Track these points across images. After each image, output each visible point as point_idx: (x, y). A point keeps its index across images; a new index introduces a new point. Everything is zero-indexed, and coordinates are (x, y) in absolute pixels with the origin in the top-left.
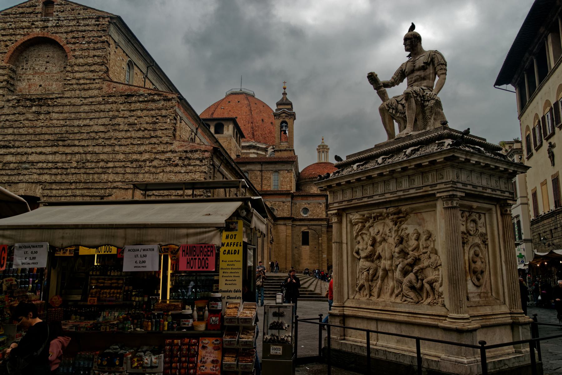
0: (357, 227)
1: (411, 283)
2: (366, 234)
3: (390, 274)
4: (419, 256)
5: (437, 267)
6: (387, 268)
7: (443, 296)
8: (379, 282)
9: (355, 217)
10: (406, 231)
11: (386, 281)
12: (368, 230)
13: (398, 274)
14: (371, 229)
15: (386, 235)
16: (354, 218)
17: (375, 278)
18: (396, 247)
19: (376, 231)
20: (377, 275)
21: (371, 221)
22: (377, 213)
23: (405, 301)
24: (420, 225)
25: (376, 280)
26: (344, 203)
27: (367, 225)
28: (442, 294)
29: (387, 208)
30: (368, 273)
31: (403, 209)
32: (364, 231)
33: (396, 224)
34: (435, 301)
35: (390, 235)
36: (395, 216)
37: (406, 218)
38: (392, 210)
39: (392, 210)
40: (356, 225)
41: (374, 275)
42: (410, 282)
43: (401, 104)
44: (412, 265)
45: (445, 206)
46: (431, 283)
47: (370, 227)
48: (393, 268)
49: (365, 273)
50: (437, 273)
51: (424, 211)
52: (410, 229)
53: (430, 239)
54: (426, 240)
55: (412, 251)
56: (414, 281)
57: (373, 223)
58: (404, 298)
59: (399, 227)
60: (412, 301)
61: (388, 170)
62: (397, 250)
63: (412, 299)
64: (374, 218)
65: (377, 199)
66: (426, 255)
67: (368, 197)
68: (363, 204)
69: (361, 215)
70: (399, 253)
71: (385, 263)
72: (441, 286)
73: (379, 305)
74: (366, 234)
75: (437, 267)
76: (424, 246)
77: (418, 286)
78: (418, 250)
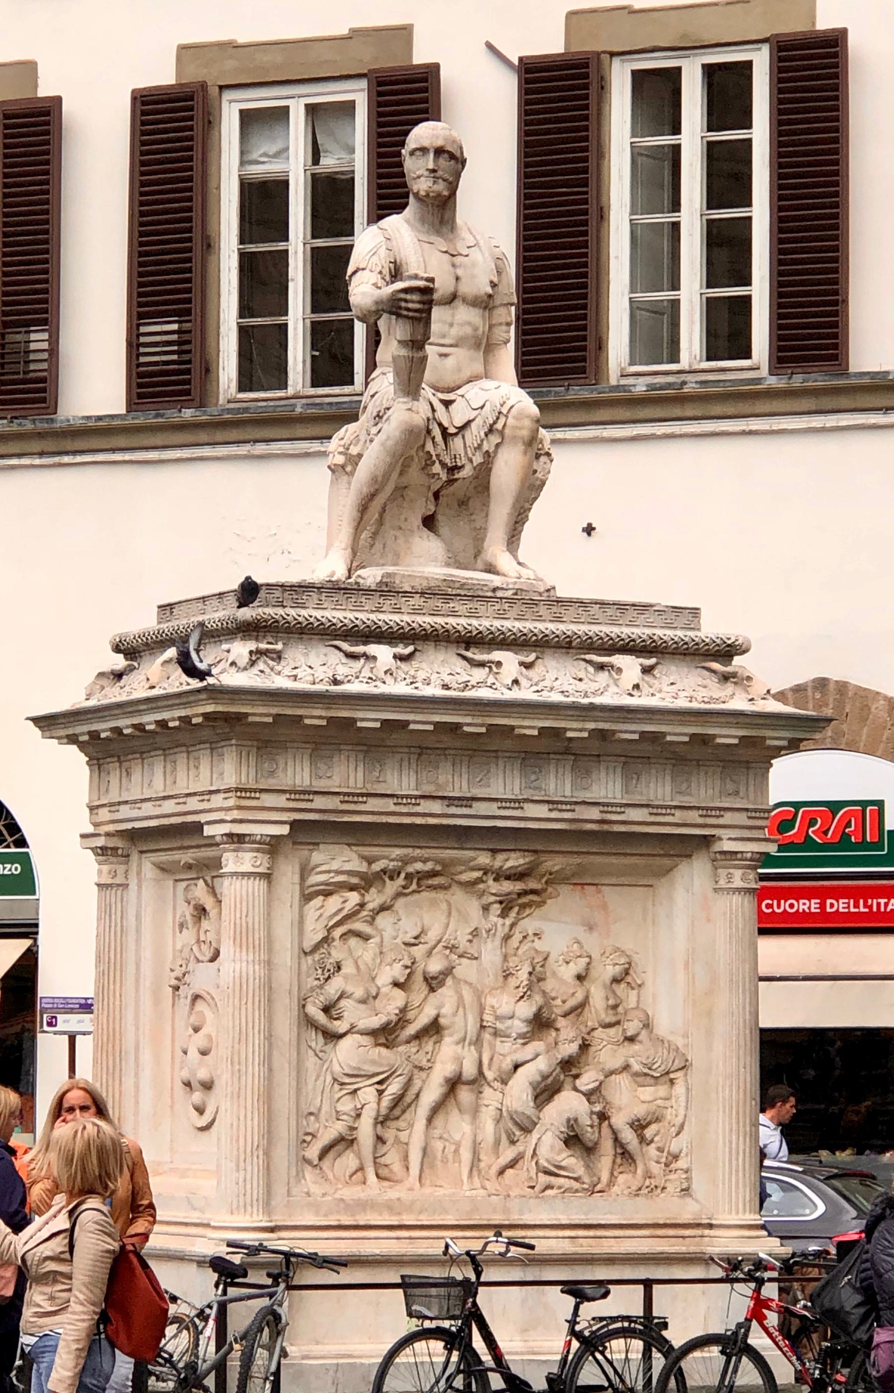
0: (334, 903)
1: (571, 1127)
2: (365, 938)
3: (465, 1095)
4: (589, 1033)
5: (668, 1073)
6: (469, 1070)
7: (682, 1164)
8: (420, 1124)
9: (337, 860)
10: (538, 944)
11: (439, 1121)
12: (372, 921)
13: (519, 1094)
14: (383, 920)
15: (452, 948)
16: (335, 866)
17: (397, 1112)
18: (522, 997)
19: (409, 929)
20: (408, 1099)
21: (392, 887)
22: (437, 861)
23: (549, 1187)
24: (591, 928)
25: (397, 1118)
26: (320, 802)
27: (374, 898)
28: (676, 1157)
29: (494, 851)
30: (380, 1093)
31: (554, 863)
32: (358, 926)
33: (504, 915)
34: (654, 1182)
35: (473, 951)
36: (518, 886)
37: (543, 895)
38: (515, 861)
39: (515, 861)
40: (327, 894)
41: (398, 1100)
42: (572, 1123)
43: (440, 425)
44: (569, 1065)
45: (738, 883)
46: (639, 1126)
47: (383, 908)
48: (489, 1075)
49: (368, 1094)
50: (662, 1090)
51: (614, 881)
52: (558, 932)
53: (629, 979)
54: (616, 980)
55: (565, 1015)
56: (585, 1120)
57: (399, 895)
58: (544, 1179)
59: (513, 925)
60: (576, 1185)
61: (591, 725)
62: (526, 1010)
63: (576, 1179)
64: (409, 877)
65: (482, 815)
66: (612, 1031)
67: (451, 800)
68: (419, 821)
69: (363, 858)
70: (529, 1022)
71: (448, 1057)
72: (678, 1134)
73: (446, 1212)
74: (365, 938)
75: (668, 1073)
76: (611, 1002)
77: (590, 1135)
78: (579, 1015)
